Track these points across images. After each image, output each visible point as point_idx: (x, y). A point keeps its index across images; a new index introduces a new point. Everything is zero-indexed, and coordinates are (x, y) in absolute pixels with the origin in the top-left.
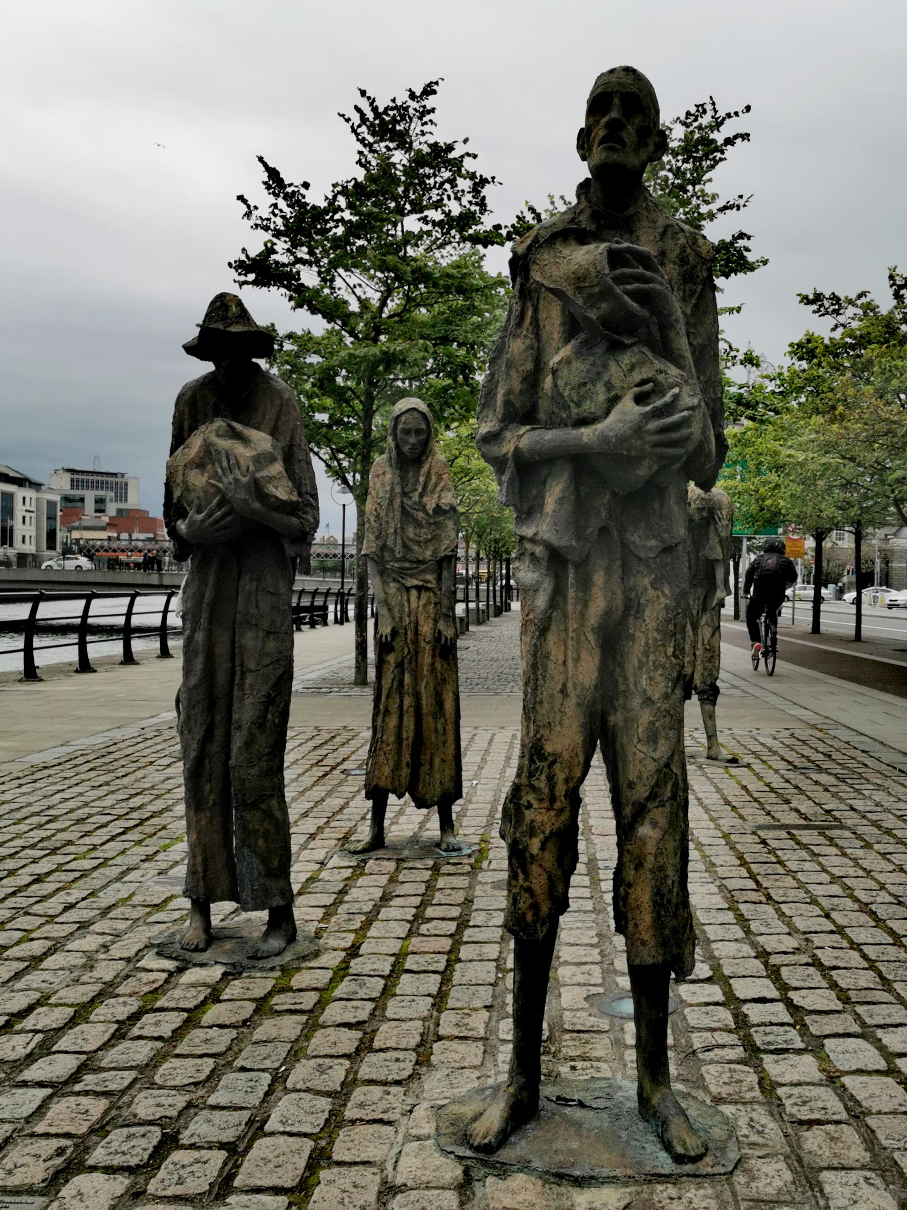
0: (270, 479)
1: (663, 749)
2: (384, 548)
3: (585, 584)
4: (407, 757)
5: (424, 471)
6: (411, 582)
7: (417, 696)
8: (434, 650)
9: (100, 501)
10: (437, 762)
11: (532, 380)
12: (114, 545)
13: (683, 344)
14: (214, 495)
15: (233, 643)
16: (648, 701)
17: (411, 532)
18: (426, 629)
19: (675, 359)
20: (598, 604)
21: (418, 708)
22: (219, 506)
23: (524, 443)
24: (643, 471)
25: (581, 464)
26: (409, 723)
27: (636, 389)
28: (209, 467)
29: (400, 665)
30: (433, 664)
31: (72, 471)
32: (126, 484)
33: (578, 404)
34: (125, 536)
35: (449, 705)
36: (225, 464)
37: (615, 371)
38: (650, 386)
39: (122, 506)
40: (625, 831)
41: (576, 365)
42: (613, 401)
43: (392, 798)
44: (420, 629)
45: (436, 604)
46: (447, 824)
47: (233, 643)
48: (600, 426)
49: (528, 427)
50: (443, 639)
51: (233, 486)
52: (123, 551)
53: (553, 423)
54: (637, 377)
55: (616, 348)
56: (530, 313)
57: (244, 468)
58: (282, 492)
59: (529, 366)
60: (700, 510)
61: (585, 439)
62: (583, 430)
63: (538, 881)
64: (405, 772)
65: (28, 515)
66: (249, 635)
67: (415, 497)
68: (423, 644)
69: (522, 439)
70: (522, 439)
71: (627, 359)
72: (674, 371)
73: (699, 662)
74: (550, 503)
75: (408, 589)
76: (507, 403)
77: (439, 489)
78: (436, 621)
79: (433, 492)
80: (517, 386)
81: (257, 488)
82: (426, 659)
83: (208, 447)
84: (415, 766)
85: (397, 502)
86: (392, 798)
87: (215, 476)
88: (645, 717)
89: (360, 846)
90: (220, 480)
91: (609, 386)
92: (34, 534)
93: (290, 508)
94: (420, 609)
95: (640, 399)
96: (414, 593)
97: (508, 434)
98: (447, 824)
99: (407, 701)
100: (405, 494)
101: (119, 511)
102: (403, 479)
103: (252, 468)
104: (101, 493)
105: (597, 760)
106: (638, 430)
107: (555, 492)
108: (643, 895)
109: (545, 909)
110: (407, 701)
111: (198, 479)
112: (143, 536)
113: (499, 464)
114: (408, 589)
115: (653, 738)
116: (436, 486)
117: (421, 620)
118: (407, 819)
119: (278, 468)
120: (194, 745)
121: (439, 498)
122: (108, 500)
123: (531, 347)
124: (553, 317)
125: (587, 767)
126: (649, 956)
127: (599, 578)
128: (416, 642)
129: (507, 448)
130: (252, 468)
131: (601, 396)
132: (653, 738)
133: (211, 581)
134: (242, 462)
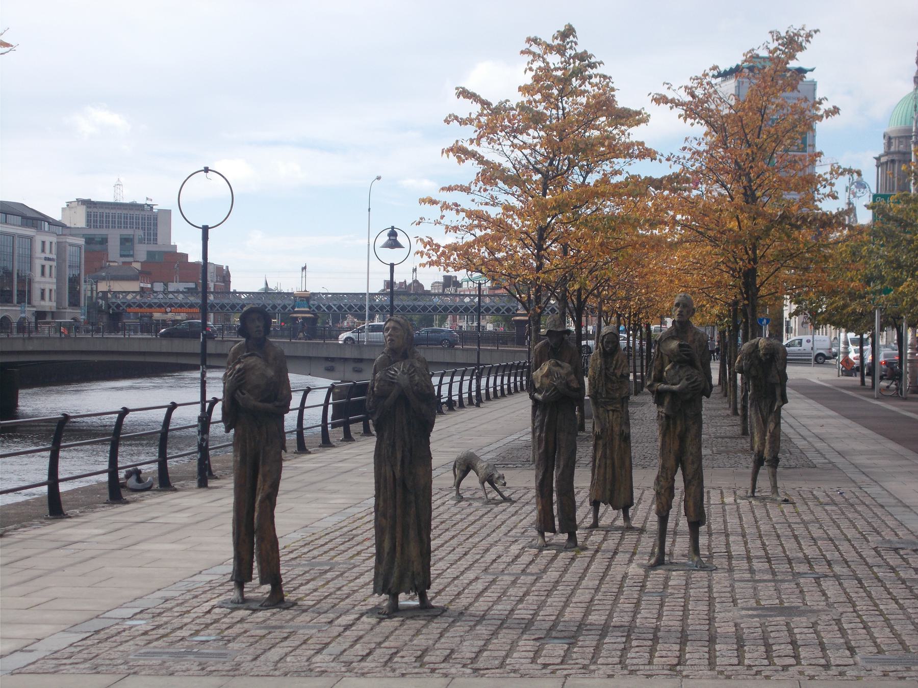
0: (571, 381)
1: (696, 466)
2: (597, 392)
3: (675, 424)
4: (608, 487)
6: (610, 408)
7: (612, 459)
9: (126, 241)
10: (622, 489)
12: (151, 299)
13: (699, 364)
15: (555, 438)
16: (691, 454)
17: (609, 386)
18: (616, 429)
19: (697, 368)
20: (679, 429)
21: (613, 464)
24: (688, 396)
25: (673, 393)
26: (609, 470)
29: (605, 445)
30: (620, 445)
31: (88, 203)
32: (156, 219)
34: (159, 287)
35: (627, 463)
37: (681, 373)
39: (152, 248)
40: (687, 487)
42: (680, 380)
43: (602, 505)
46: (627, 518)
47: (555, 438)
52: (160, 306)
53: (666, 383)
58: (575, 385)
60: (764, 354)
63: (664, 500)
64: (608, 493)
65: (47, 264)
67: (612, 370)
71: (684, 369)
72: (696, 371)
73: (767, 444)
74: (666, 403)
75: (608, 411)
76: (654, 377)
78: (621, 425)
81: (567, 384)
82: (616, 442)
83: (549, 370)
84: (612, 492)
85: (603, 374)
86: (602, 505)
87: (552, 380)
88: (691, 458)
89: (588, 525)
92: (54, 287)
96: (611, 413)
98: (627, 518)
99: (608, 462)
100: (606, 368)
101: (150, 254)
102: (606, 362)
104: (128, 232)
105: (679, 471)
106: (687, 387)
108: (691, 504)
109: (666, 508)
110: (608, 462)
112: (182, 286)
113: (653, 392)
114: (608, 411)
115: (693, 463)
117: (614, 425)
118: (608, 515)
119: (573, 376)
120: (541, 474)
122: (136, 241)
124: (666, 359)
125: (676, 471)
126: (693, 519)
127: (678, 422)
129: (655, 389)
132: (693, 463)
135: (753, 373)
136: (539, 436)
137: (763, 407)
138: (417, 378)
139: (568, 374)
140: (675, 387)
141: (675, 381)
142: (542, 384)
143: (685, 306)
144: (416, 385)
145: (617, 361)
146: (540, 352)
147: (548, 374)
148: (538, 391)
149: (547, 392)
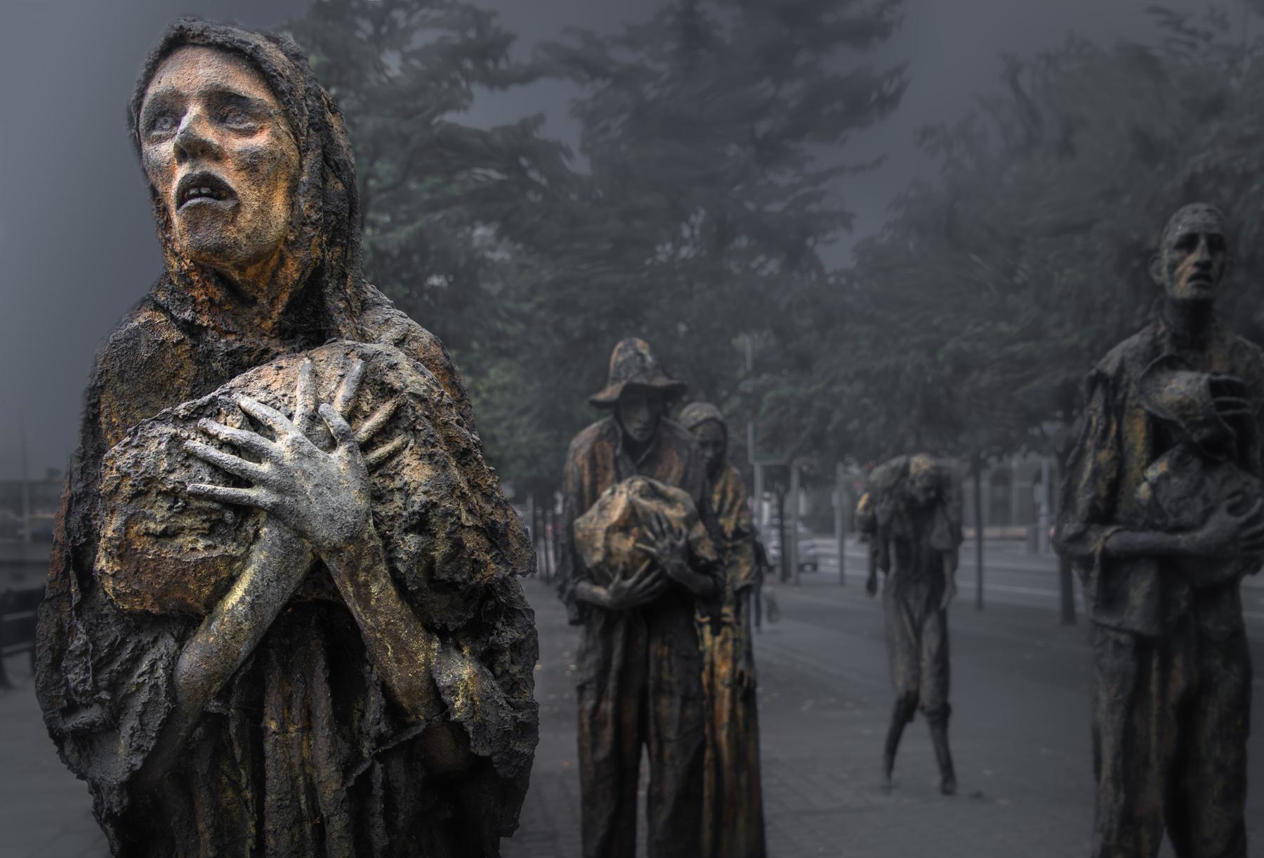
5: (718, 487)
8: (733, 694)
11: (1116, 487)
14: (643, 560)
22: (648, 571)
23: (1113, 543)
27: (1229, 502)
28: (635, 530)
33: (1177, 515)
36: (657, 528)
37: (1211, 485)
38: (1238, 498)
41: (1174, 480)
42: (1208, 513)
44: (717, 670)
45: (735, 640)
48: (1200, 535)
49: (1113, 529)
50: (745, 683)
51: (668, 552)
53: (1130, 526)
54: (1228, 489)
55: (1209, 464)
56: (1114, 427)
57: (677, 531)
59: (1114, 474)
61: (1183, 545)
62: (1179, 536)
66: (665, 701)
68: (720, 688)
69: (1104, 539)
70: (1104, 539)
71: (1219, 475)
77: (736, 508)
78: (735, 661)
79: (730, 512)
80: (1103, 493)
81: (689, 551)
87: (642, 538)
90: (652, 544)
91: (1206, 499)
93: (709, 568)
94: (717, 647)
95: (1233, 510)
97: (1093, 535)
103: (685, 531)
107: (1140, 589)
111: (625, 545)
116: (733, 504)
119: (700, 529)
121: (738, 519)
123: (1115, 458)
128: (711, 685)
130: (685, 531)
131: (1200, 507)
133: (618, 647)
134: (675, 524)
135: (897, 529)
136: (596, 708)
137: (911, 601)
138: (415, 472)
139: (689, 522)
140: (1183, 540)
141: (1187, 517)
142: (609, 554)
143: (1216, 244)
144: (421, 524)
145: (724, 494)
146: (592, 457)
147: (632, 520)
148: (599, 575)
149: (625, 576)
